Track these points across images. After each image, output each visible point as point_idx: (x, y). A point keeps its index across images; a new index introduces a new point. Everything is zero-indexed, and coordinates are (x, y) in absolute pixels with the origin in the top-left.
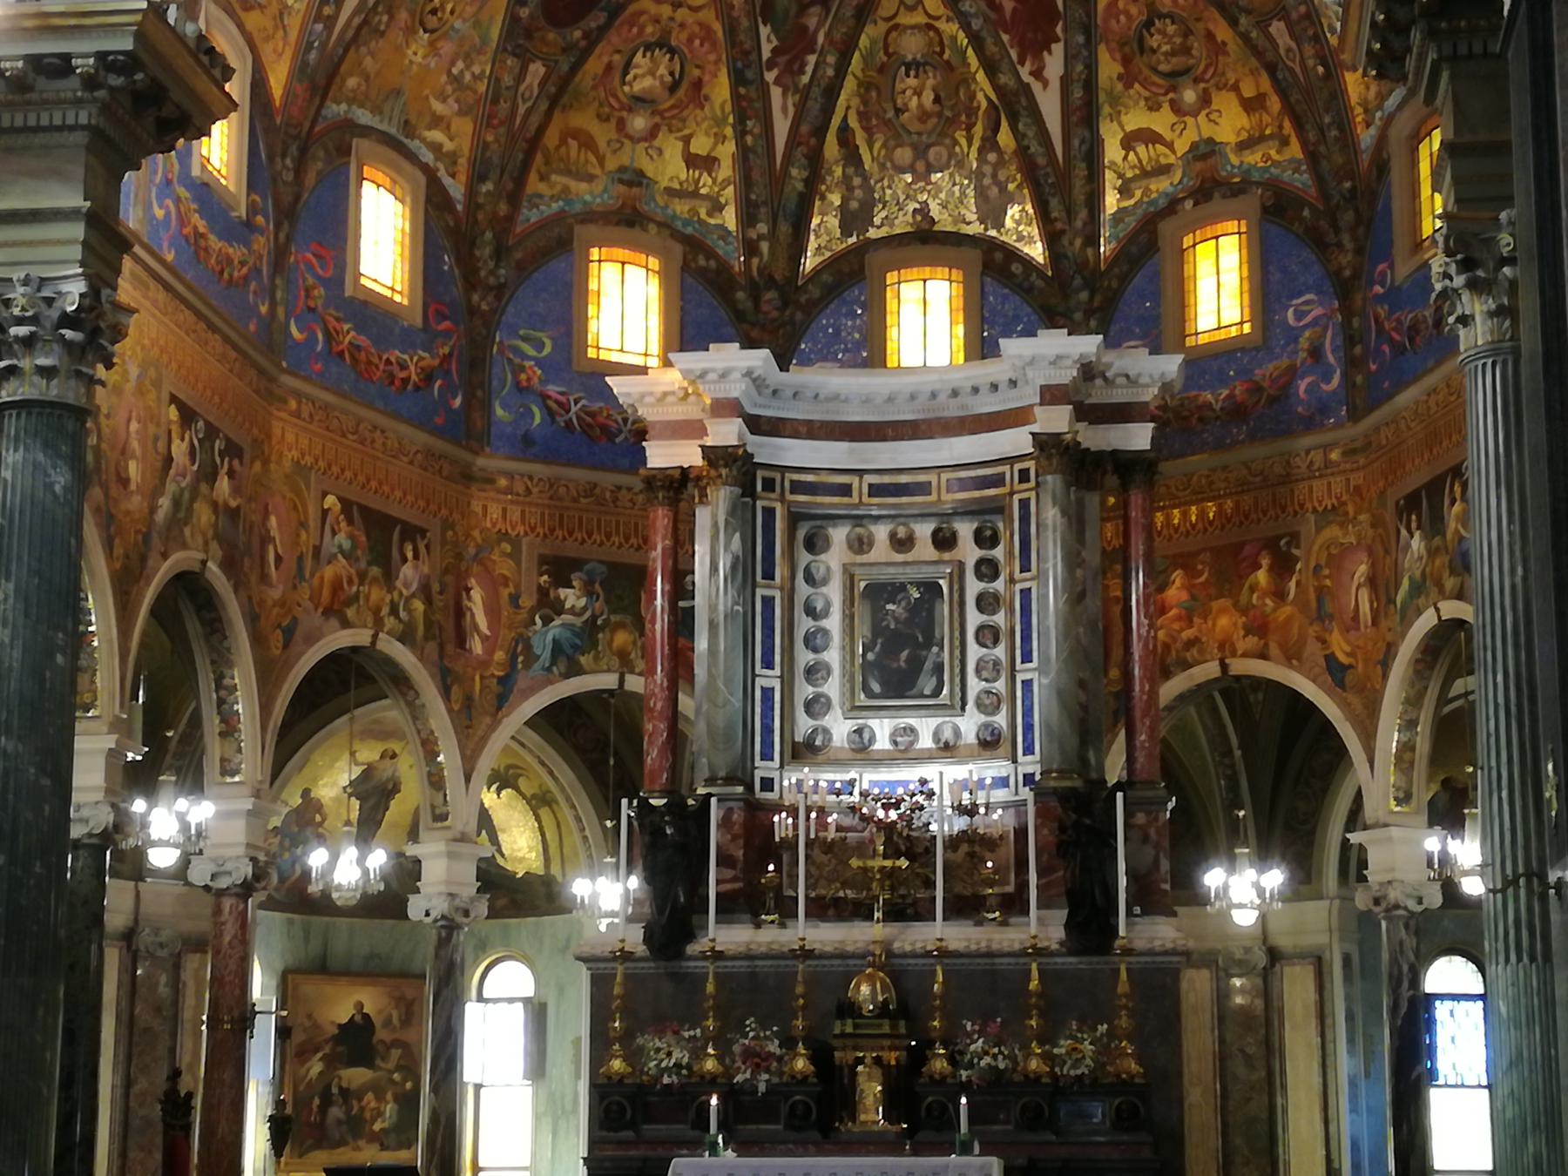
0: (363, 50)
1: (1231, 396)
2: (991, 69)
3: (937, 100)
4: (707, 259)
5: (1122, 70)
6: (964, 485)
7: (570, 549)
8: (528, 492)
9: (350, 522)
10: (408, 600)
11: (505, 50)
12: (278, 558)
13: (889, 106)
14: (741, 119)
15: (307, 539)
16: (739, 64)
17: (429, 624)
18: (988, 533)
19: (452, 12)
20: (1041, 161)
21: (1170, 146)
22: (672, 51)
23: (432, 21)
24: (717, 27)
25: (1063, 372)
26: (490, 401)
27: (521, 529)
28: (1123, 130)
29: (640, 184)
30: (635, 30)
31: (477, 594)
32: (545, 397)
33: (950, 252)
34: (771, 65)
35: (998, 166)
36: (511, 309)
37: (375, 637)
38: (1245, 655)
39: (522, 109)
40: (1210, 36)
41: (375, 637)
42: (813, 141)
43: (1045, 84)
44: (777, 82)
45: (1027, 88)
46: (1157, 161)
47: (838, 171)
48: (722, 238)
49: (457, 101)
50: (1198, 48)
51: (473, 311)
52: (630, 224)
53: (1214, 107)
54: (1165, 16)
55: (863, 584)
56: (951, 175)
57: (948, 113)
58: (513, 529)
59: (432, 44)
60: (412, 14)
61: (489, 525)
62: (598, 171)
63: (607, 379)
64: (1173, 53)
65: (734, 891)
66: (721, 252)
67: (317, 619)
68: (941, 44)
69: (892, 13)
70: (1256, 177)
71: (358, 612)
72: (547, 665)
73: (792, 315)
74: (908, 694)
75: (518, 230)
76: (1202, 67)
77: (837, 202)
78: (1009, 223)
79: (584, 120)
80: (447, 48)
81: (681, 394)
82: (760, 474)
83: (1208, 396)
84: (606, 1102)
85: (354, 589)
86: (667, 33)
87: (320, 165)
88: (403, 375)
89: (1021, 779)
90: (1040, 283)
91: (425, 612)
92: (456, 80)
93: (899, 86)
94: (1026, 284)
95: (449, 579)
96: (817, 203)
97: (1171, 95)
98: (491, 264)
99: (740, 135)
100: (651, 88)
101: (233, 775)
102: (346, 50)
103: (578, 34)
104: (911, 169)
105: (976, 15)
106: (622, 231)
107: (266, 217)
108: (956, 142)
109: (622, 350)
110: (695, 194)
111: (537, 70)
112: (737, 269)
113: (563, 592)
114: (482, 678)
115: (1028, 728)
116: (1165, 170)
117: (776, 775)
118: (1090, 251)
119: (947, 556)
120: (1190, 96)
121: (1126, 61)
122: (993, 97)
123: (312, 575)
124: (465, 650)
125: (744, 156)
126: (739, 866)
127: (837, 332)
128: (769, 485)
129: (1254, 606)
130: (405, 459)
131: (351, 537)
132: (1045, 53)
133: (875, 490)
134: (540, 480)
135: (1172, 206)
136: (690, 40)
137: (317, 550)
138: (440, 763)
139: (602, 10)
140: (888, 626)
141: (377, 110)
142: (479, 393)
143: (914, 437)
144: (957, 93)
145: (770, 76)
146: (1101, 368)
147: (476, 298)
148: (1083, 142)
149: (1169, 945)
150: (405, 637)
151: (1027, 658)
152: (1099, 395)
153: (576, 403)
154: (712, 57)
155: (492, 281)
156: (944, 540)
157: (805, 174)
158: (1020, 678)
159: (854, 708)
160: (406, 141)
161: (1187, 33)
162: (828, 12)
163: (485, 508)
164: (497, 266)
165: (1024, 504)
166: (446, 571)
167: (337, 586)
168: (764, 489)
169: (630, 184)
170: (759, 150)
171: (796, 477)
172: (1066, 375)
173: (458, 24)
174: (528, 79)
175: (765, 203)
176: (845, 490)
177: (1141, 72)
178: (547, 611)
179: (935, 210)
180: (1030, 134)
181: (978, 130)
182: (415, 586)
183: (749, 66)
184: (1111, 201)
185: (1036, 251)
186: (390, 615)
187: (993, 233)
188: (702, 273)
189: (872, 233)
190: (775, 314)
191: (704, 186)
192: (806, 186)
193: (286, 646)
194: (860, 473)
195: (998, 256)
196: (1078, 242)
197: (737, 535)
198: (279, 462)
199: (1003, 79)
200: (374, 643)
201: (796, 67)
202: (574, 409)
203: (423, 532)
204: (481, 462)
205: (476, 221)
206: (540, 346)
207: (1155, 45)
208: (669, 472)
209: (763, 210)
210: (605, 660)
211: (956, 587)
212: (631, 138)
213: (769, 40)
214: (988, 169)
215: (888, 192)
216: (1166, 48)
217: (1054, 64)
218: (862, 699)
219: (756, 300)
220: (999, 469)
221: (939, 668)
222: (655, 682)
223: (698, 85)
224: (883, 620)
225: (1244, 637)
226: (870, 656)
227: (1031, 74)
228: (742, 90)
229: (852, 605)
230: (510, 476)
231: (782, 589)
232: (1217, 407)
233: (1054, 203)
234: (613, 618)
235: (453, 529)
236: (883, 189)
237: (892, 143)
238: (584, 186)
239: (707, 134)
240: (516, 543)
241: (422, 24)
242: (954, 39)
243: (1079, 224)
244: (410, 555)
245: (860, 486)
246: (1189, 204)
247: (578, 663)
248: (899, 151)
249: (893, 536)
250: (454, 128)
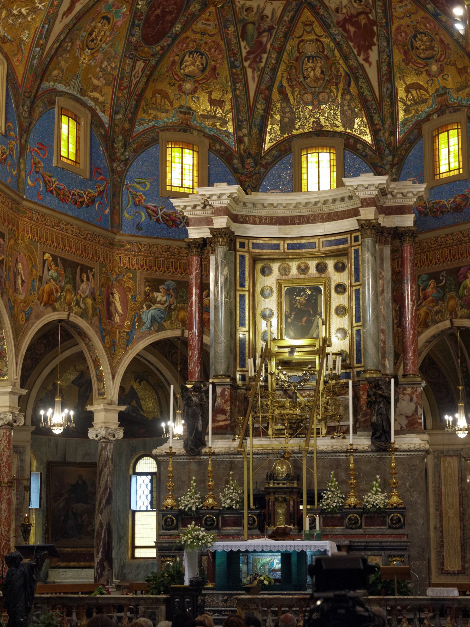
0: (60, 58)
1: (454, 201)
2: (346, 58)
3: (322, 72)
4: (221, 146)
5: (404, 57)
6: (330, 243)
7: (159, 275)
8: (140, 250)
9: (57, 265)
10: (84, 299)
11: (126, 56)
12: (23, 282)
13: (301, 76)
14: (234, 84)
15: (36, 273)
16: (232, 59)
17: (94, 309)
18: (340, 265)
19: (101, 41)
20: (369, 98)
21: (427, 90)
22: (202, 54)
23: (92, 45)
24: (221, 43)
26: (122, 210)
27: (136, 267)
28: (405, 83)
29: (189, 113)
30: (185, 45)
31: (117, 296)
32: (147, 208)
33: (329, 140)
34: (246, 59)
35: (350, 101)
36: (131, 169)
37: (69, 315)
38: (461, 317)
39: (134, 82)
40: (442, 41)
41: (69, 315)
42: (267, 92)
43: (370, 64)
44: (250, 66)
45: (362, 66)
46: (421, 97)
47: (279, 105)
48: (227, 136)
49: (105, 79)
50: (437, 47)
51: (113, 171)
52: (185, 131)
53: (445, 73)
54: (422, 33)
55: (286, 288)
56: (329, 105)
57: (328, 78)
58: (133, 267)
59: (92, 54)
60: (83, 42)
61: (122, 265)
62: (170, 108)
63: (172, 200)
64: (426, 49)
65: (226, 425)
66: (227, 142)
67: (42, 308)
68: (323, 47)
69: (300, 35)
70: (464, 103)
71: (60, 305)
72: (149, 326)
73: (259, 169)
75: (134, 135)
76: (439, 56)
77: (279, 119)
78: (356, 126)
79: (163, 86)
80: (99, 56)
81: (202, 205)
82: (238, 241)
83: (444, 201)
84: (165, 518)
85: (59, 294)
86: (199, 46)
87: (41, 109)
88: (80, 200)
90: (370, 153)
91: (92, 304)
92: (103, 70)
93: (305, 67)
94: (364, 154)
95: (104, 289)
96: (270, 119)
97: (426, 68)
98: (122, 150)
99: (234, 90)
100: (194, 71)
101: (3, 376)
102: (52, 59)
103: (158, 48)
104: (312, 103)
105: (337, 35)
106: (181, 135)
107: (15, 133)
108: (331, 91)
109: (182, 187)
110: (215, 117)
111: (141, 64)
112: (234, 150)
113: (156, 294)
114: (119, 332)
116: (424, 101)
118: (392, 138)
119: (323, 275)
120: (434, 68)
121: (406, 53)
122: (347, 70)
123: (39, 289)
124: (111, 320)
125: (236, 98)
126: (228, 414)
127: (279, 177)
128: (242, 245)
129: (465, 295)
130: (82, 237)
131: (57, 271)
132: (369, 51)
133: (291, 247)
134: (145, 245)
135: (428, 118)
136: (210, 49)
137: (41, 278)
138: (101, 370)
139: (169, 37)
140: (297, 307)
141: (67, 84)
142: (117, 207)
143: (308, 222)
144: (331, 68)
145: (246, 64)
146: (390, 190)
147: (115, 165)
148: (388, 89)
149: (417, 447)
150: (83, 315)
152: (389, 202)
153: (161, 210)
154: (220, 56)
155: (122, 158)
156: (321, 268)
157: (264, 107)
160: (82, 98)
161: (432, 40)
162: (271, 35)
163: (120, 257)
164: (125, 151)
165: (357, 252)
166: (102, 286)
167: (50, 293)
168: (240, 247)
169: (185, 113)
170: (243, 97)
171: (255, 241)
172: (373, 193)
173: (104, 46)
174: (137, 69)
175: (246, 120)
176: (277, 247)
177: (412, 58)
178: (148, 303)
179: (322, 120)
180: (364, 86)
181: (341, 85)
182: (88, 292)
183: (237, 60)
184: (401, 115)
185: (368, 139)
186: (75, 306)
187: (349, 131)
188: (218, 151)
189: (295, 132)
190: (251, 169)
191: (218, 113)
192: (264, 112)
193: (27, 320)
194: (284, 239)
195: (351, 141)
196: (387, 134)
197: (226, 268)
198: (23, 240)
199: (352, 62)
200: (68, 318)
201: (258, 60)
202: (160, 213)
203: (91, 269)
204: (118, 237)
205: (114, 132)
206: (144, 186)
207: (418, 46)
209: (245, 123)
210: (175, 324)
211: (327, 289)
212: (185, 93)
213: (245, 48)
214: (346, 102)
215: (302, 114)
216: (423, 47)
217: (374, 55)
219: (243, 162)
220: (346, 236)
222: (192, 333)
223: (214, 69)
224: (294, 304)
225: (461, 309)
227: (364, 60)
228: (234, 71)
229: (281, 297)
230: (131, 243)
231: (248, 291)
232: (449, 207)
233: (376, 117)
234: (179, 305)
235: (105, 268)
236: (299, 112)
237: (303, 92)
238: (164, 115)
239: (219, 90)
240: (134, 273)
241: (87, 46)
242: (329, 45)
243: (387, 126)
244: (85, 279)
245: (284, 246)
246: (435, 116)
247: (163, 325)
248: (306, 95)
249: (299, 268)
250: (103, 91)
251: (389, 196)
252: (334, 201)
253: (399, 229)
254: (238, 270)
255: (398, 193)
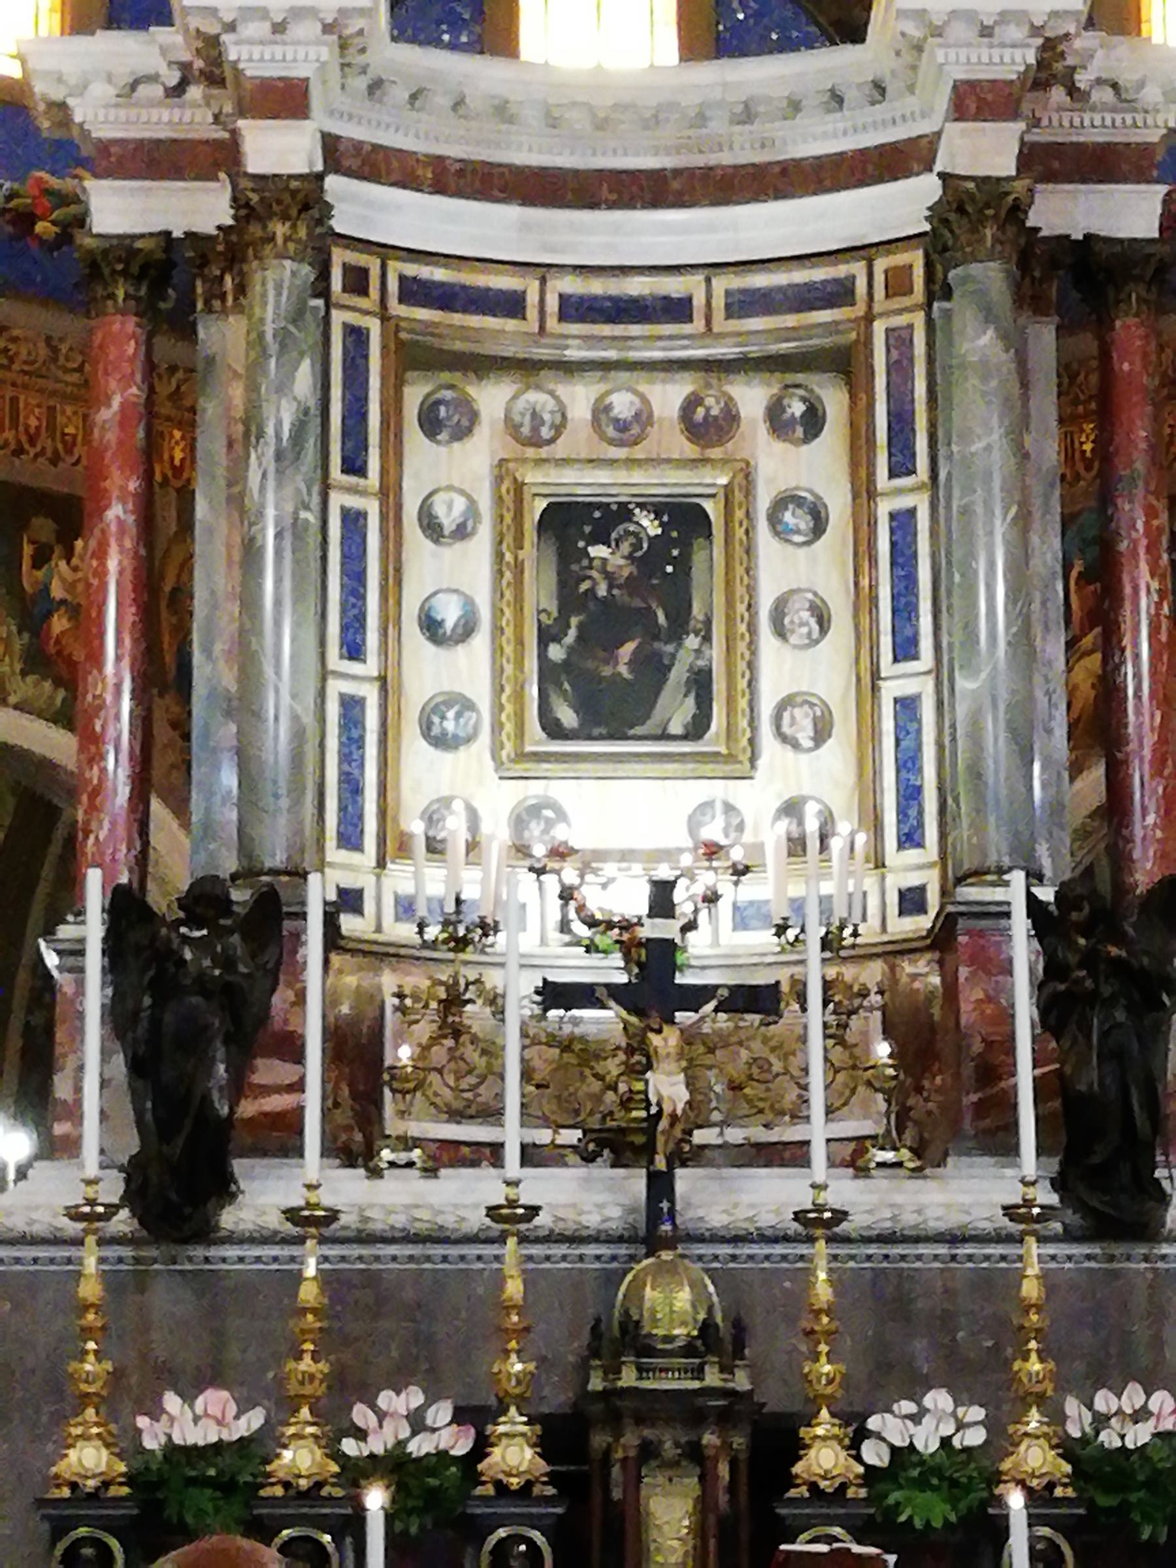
25: (1007, 54)
55: (541, 505)
74: (632, 732)
82: (340, 257)
89: (893, 899)
115: (910, 795)
117: (365, 881)
119: (715, 453)
140: (592, 591)
151: (905, 650)
158: (890, 691)
159: (521, 756)
171: (412, 269)
176: (512, 305)
194: (543, 271)
208: (139, 244)
218: (536, 739)
220: (841, 270)
221: (701, 683)
226: (556, 652)
249: (601, 411)
251: (1058, 94)
252: (795, 106)
253: (1097, 247)
254: (336, 392)
255: (1099, 81)
